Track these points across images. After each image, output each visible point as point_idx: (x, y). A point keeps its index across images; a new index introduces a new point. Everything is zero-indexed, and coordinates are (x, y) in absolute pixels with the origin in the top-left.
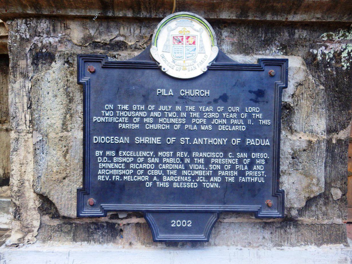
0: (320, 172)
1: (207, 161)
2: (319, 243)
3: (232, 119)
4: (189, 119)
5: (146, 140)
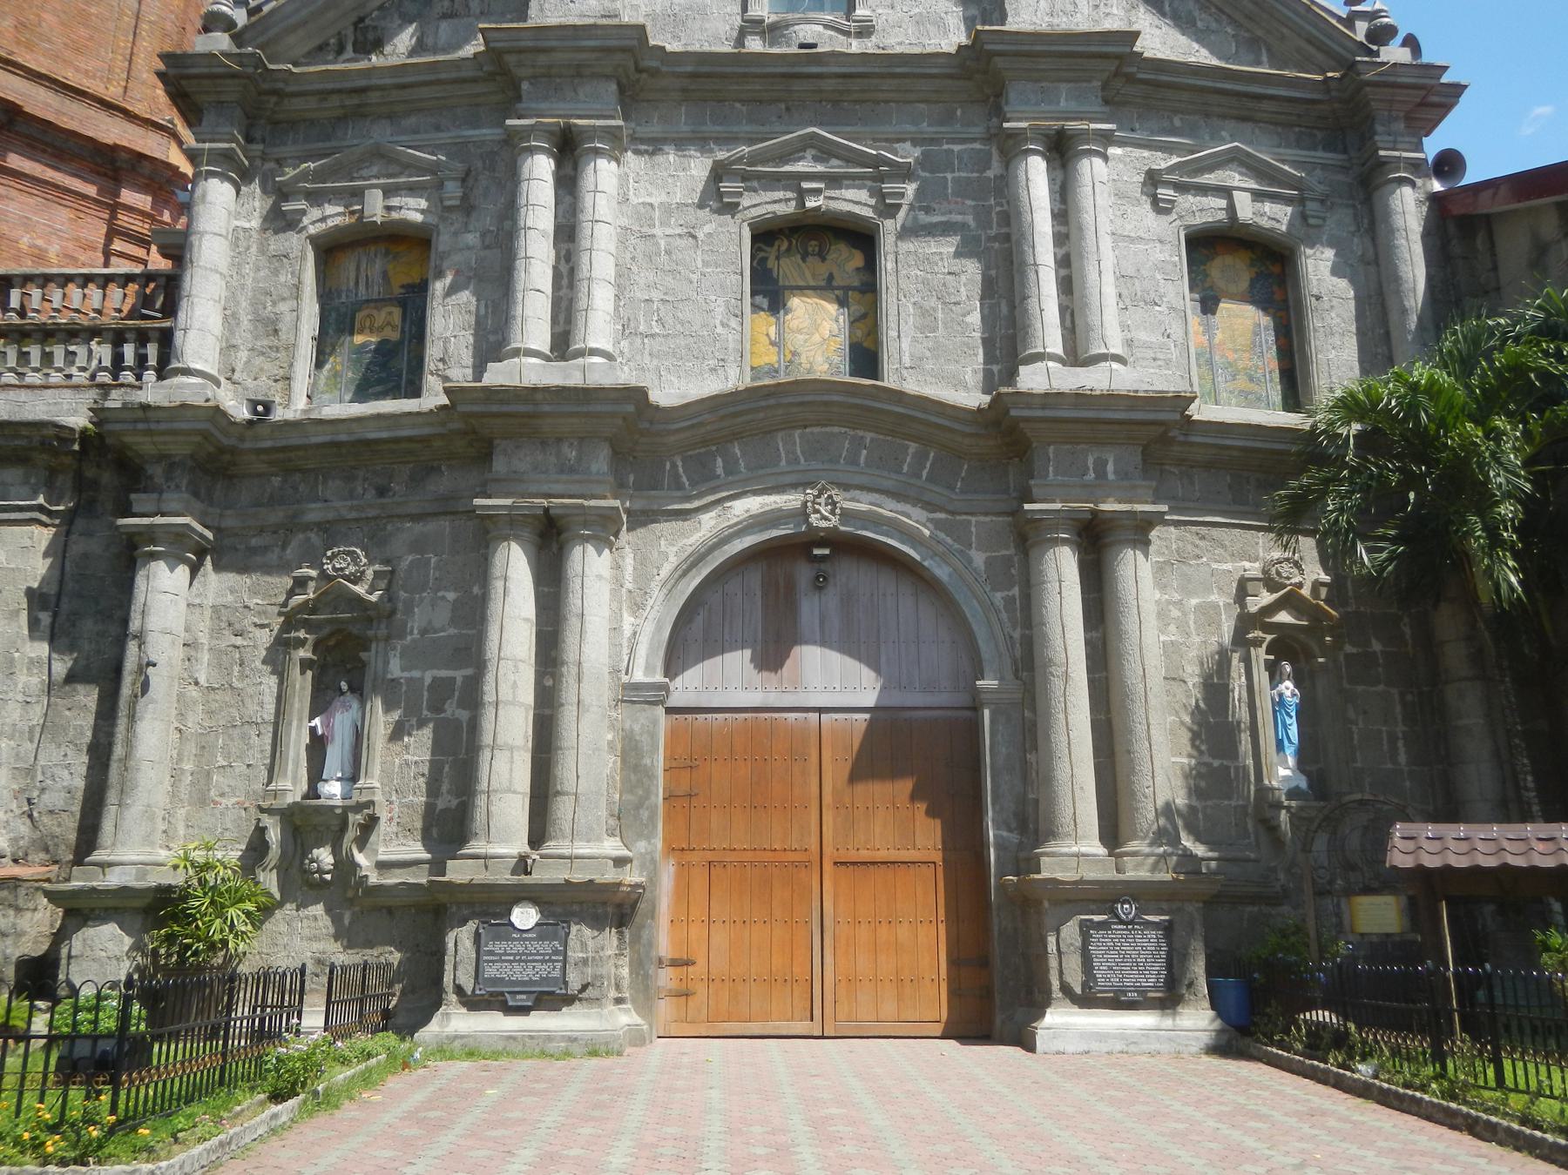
3: (546, 947)
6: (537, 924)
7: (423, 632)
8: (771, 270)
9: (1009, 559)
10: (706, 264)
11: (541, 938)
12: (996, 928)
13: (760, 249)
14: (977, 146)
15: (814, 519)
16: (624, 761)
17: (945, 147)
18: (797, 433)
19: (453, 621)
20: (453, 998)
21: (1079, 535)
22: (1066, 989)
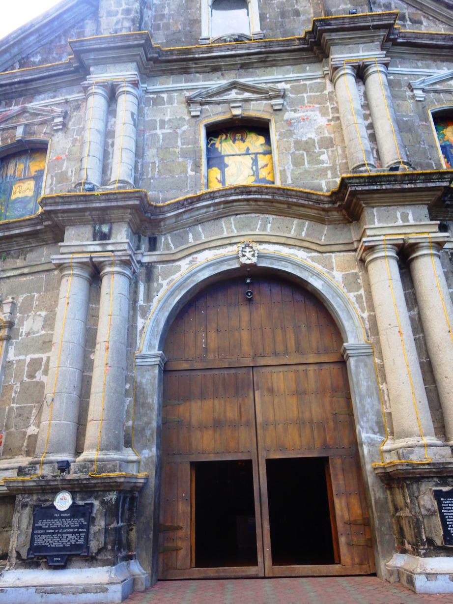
0: (102, 539)
1: (67, 537)
2: (103, 566)
3: (75, 523)
4: (63, 524)
5: (50, 531)
6: (71, 507)
7: (28, 334)
8: (217, 149)
9: (356, 274)
10: (182, 144)
11: (73, 516)
12: (373, 499)
13: (212, 140)
14: (318, 80)
15: (244, 260)
16: (136, 400)
17: (302, 83)
18: (232, 219)
19: (43, 328)
20: (14, 561)
21: (398, 254)
22: (430, 541)
